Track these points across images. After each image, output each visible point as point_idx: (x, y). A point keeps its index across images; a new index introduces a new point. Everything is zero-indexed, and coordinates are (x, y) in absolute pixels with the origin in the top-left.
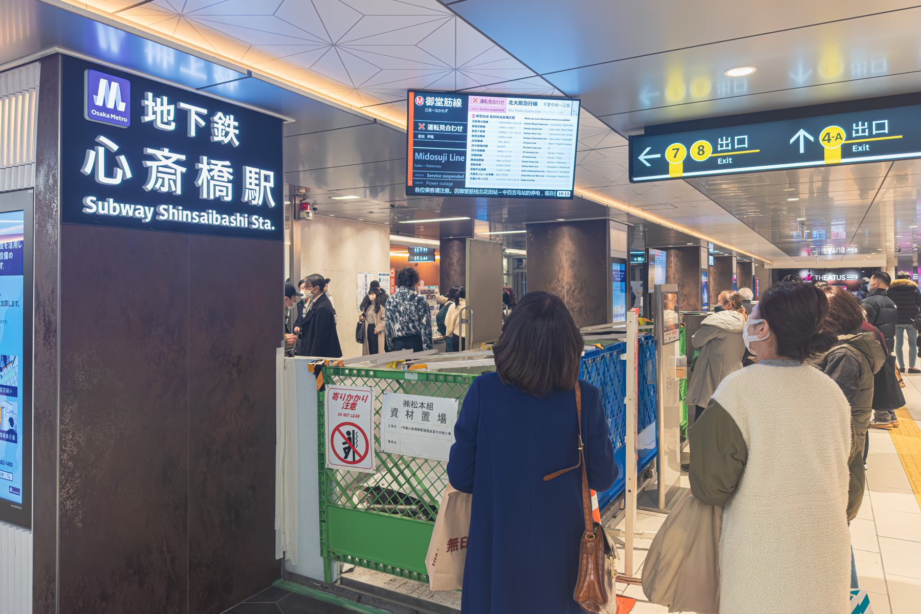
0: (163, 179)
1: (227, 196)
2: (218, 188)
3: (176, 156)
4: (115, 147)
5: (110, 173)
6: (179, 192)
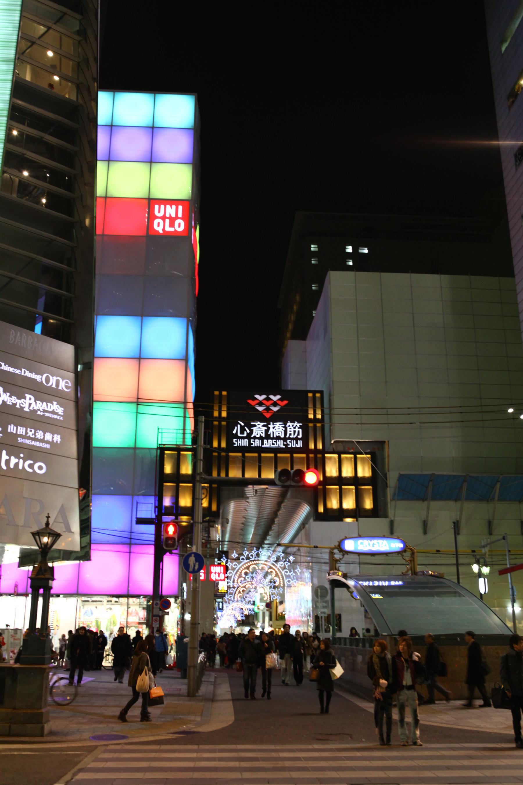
3: (262, 424)
4: (243, 424)
5: (242, 433)
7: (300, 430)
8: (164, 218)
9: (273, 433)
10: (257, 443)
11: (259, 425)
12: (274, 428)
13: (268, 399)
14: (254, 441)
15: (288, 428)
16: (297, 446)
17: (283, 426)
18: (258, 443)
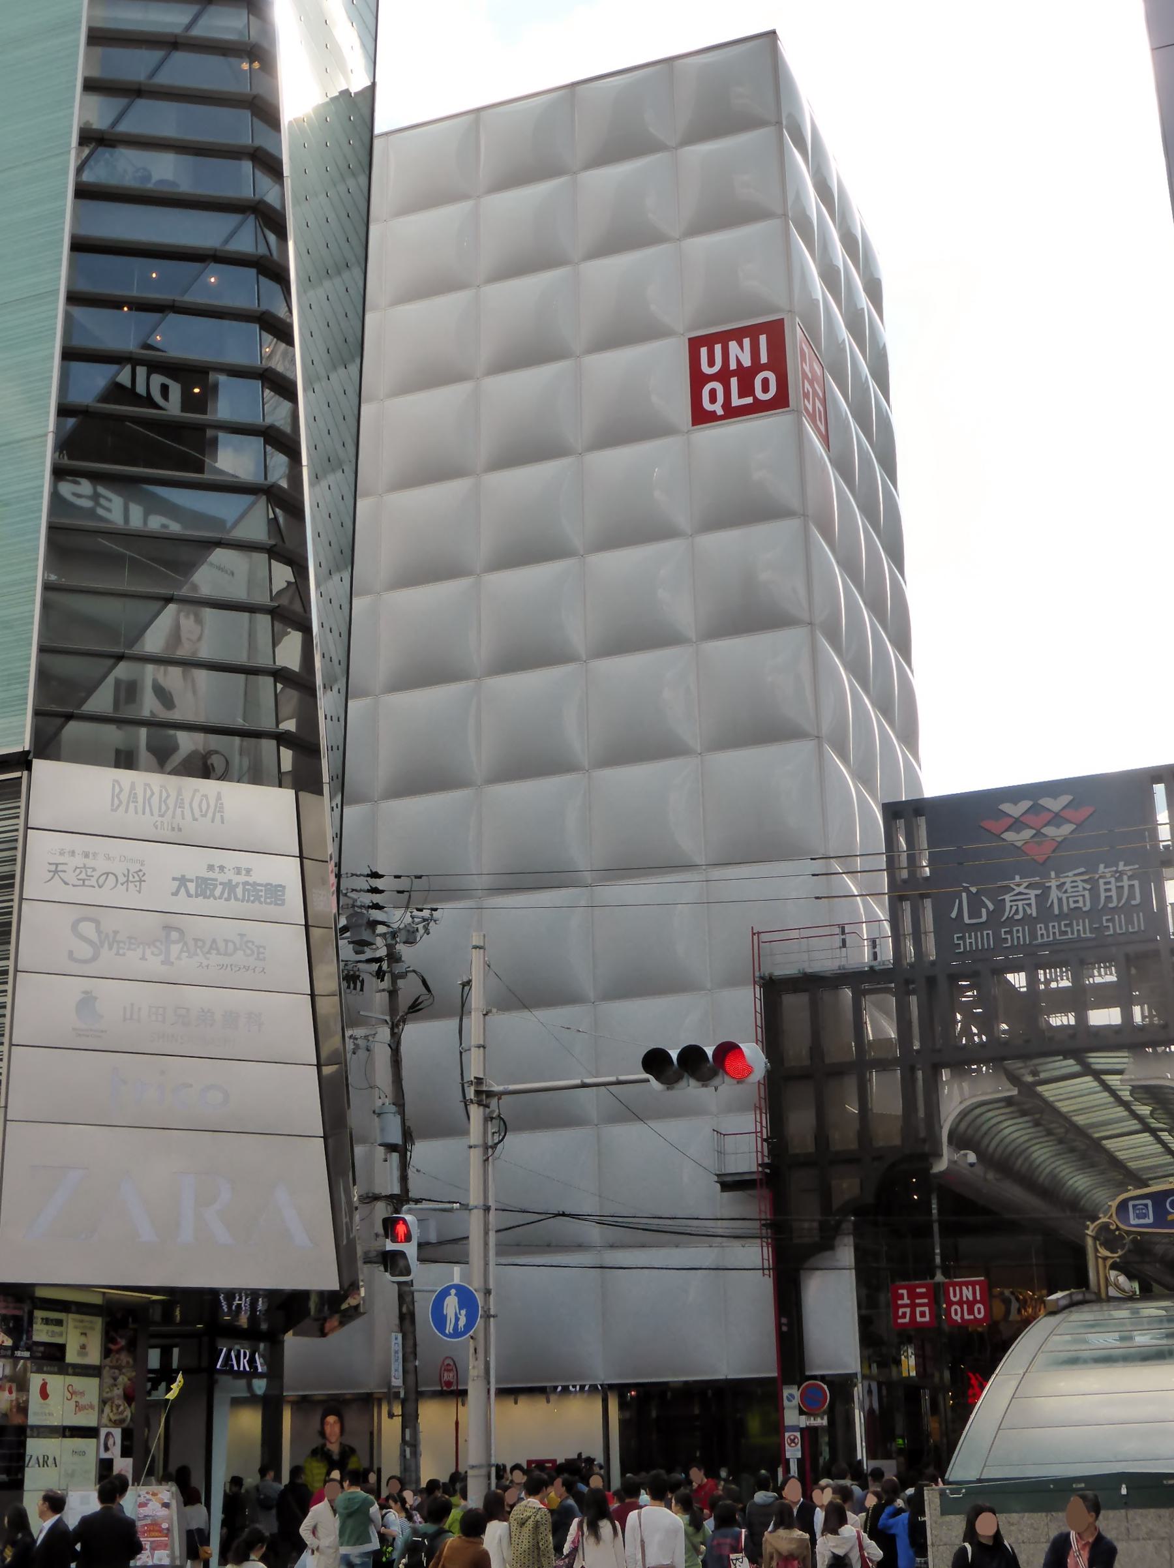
0: (1017, 905)
1: (1085, 906)
2: (1071, 900)
6: (1034, 914)
7: (1136, 883)
8: (723, 376)
9: (1060, 900)
10: (1020, 934)
11: (1018, 885)
12: (1059, 887)
13: (1035, 809)
14: (1010, 932)
15: (1101, 881)
16: (1131, 930)
17: (1086, 877)
18: (1020, 935)
